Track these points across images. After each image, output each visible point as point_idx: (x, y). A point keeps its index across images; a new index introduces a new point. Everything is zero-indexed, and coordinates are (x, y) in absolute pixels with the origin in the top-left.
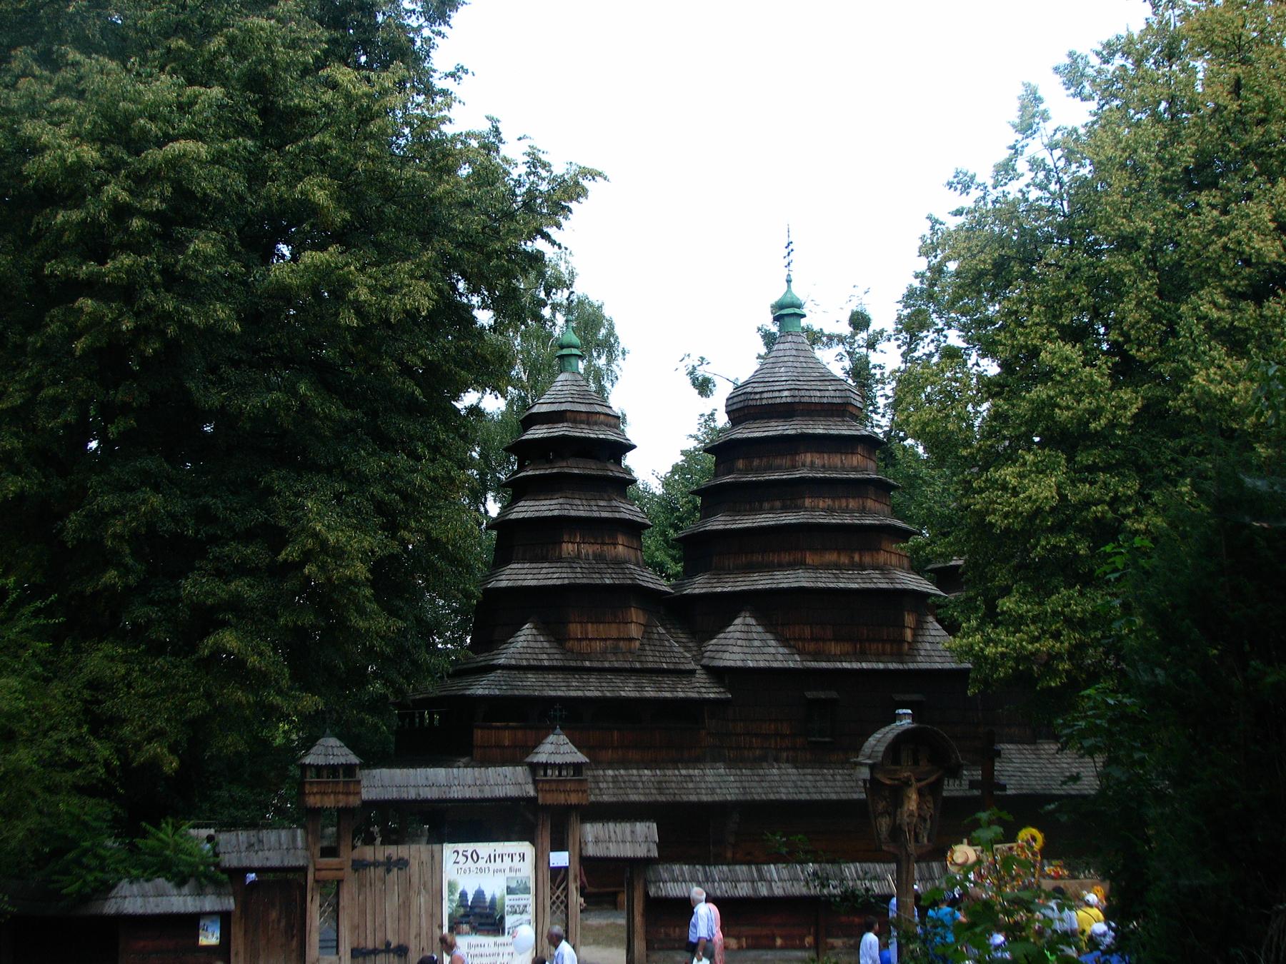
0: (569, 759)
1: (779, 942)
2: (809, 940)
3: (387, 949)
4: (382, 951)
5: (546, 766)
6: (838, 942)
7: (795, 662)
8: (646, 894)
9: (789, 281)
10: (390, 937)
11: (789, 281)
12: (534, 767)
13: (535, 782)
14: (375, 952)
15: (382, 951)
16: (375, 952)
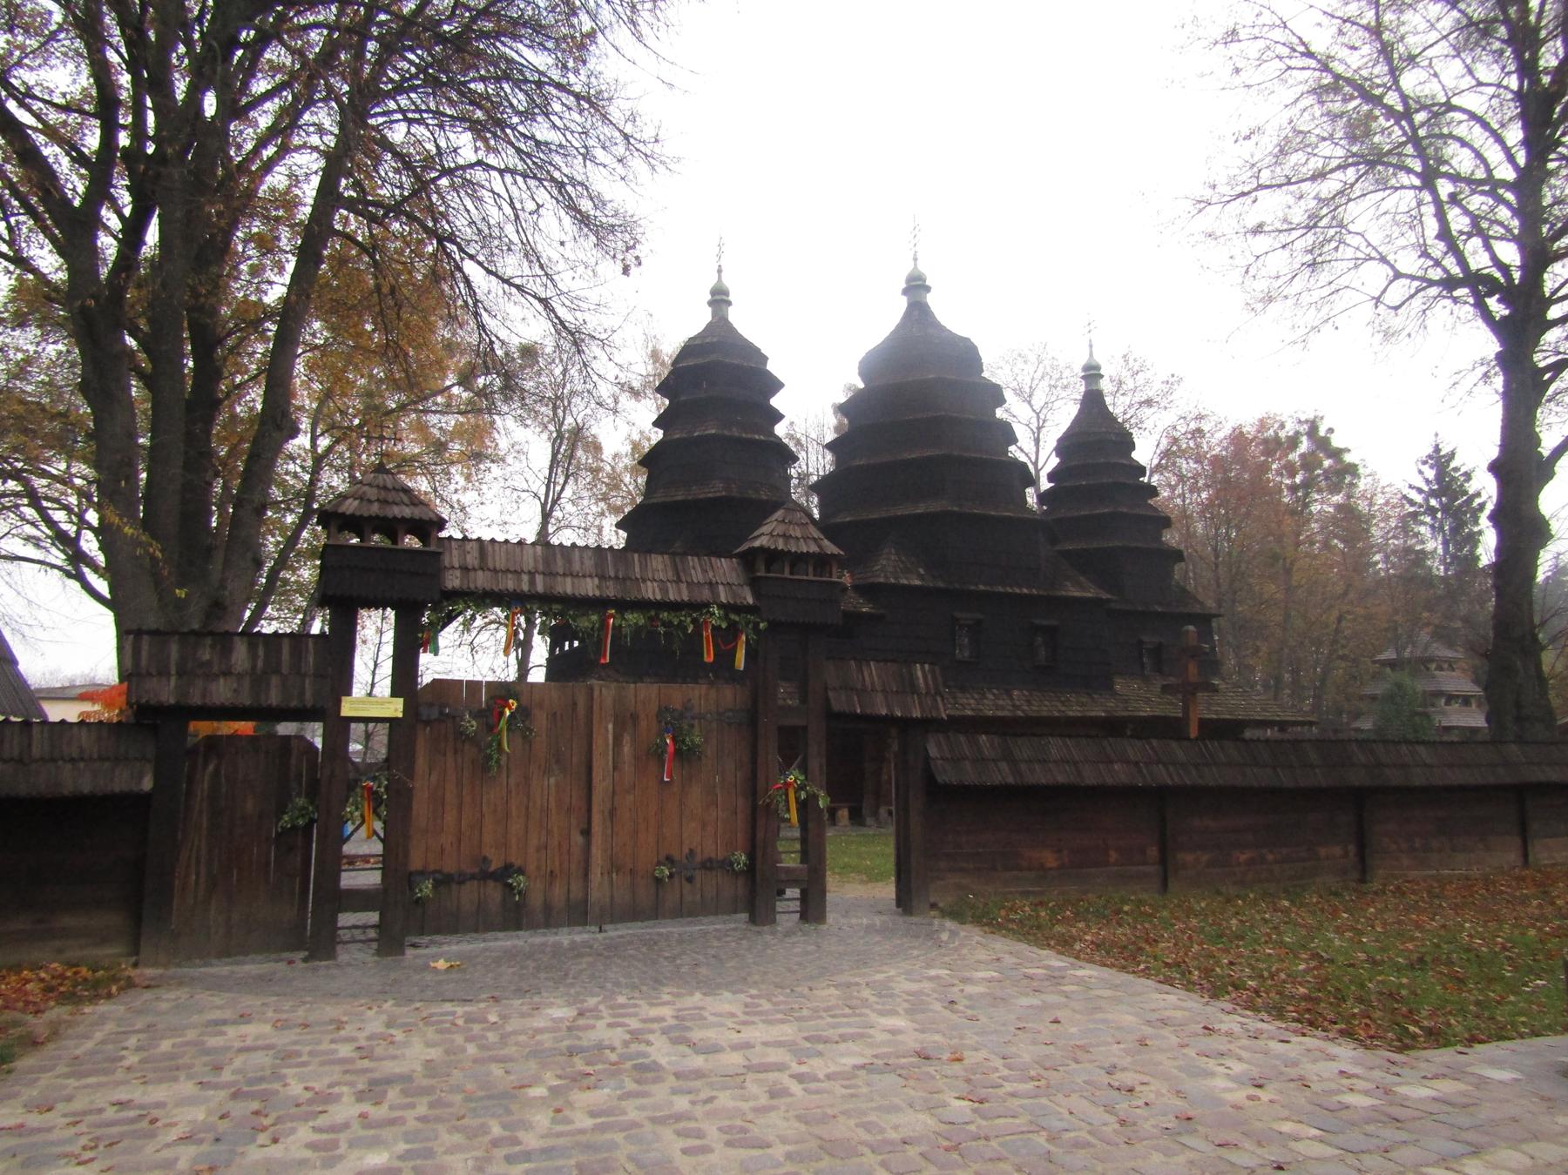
0: (813, 548)
1: (1113, 856)
2: (1153, 852)
3: (485, 876)
4: (473, 877)
5: (772, 557)
6: (1189, 858)
7: (941, 584)
8: (930, 778)
9: (915, 259)
10: (489, 852)
11: (915, 259)
12: (749, 559)
13: (754, 583)
14: (462, 879)
15: (473, 877)
16: (462, 879)
